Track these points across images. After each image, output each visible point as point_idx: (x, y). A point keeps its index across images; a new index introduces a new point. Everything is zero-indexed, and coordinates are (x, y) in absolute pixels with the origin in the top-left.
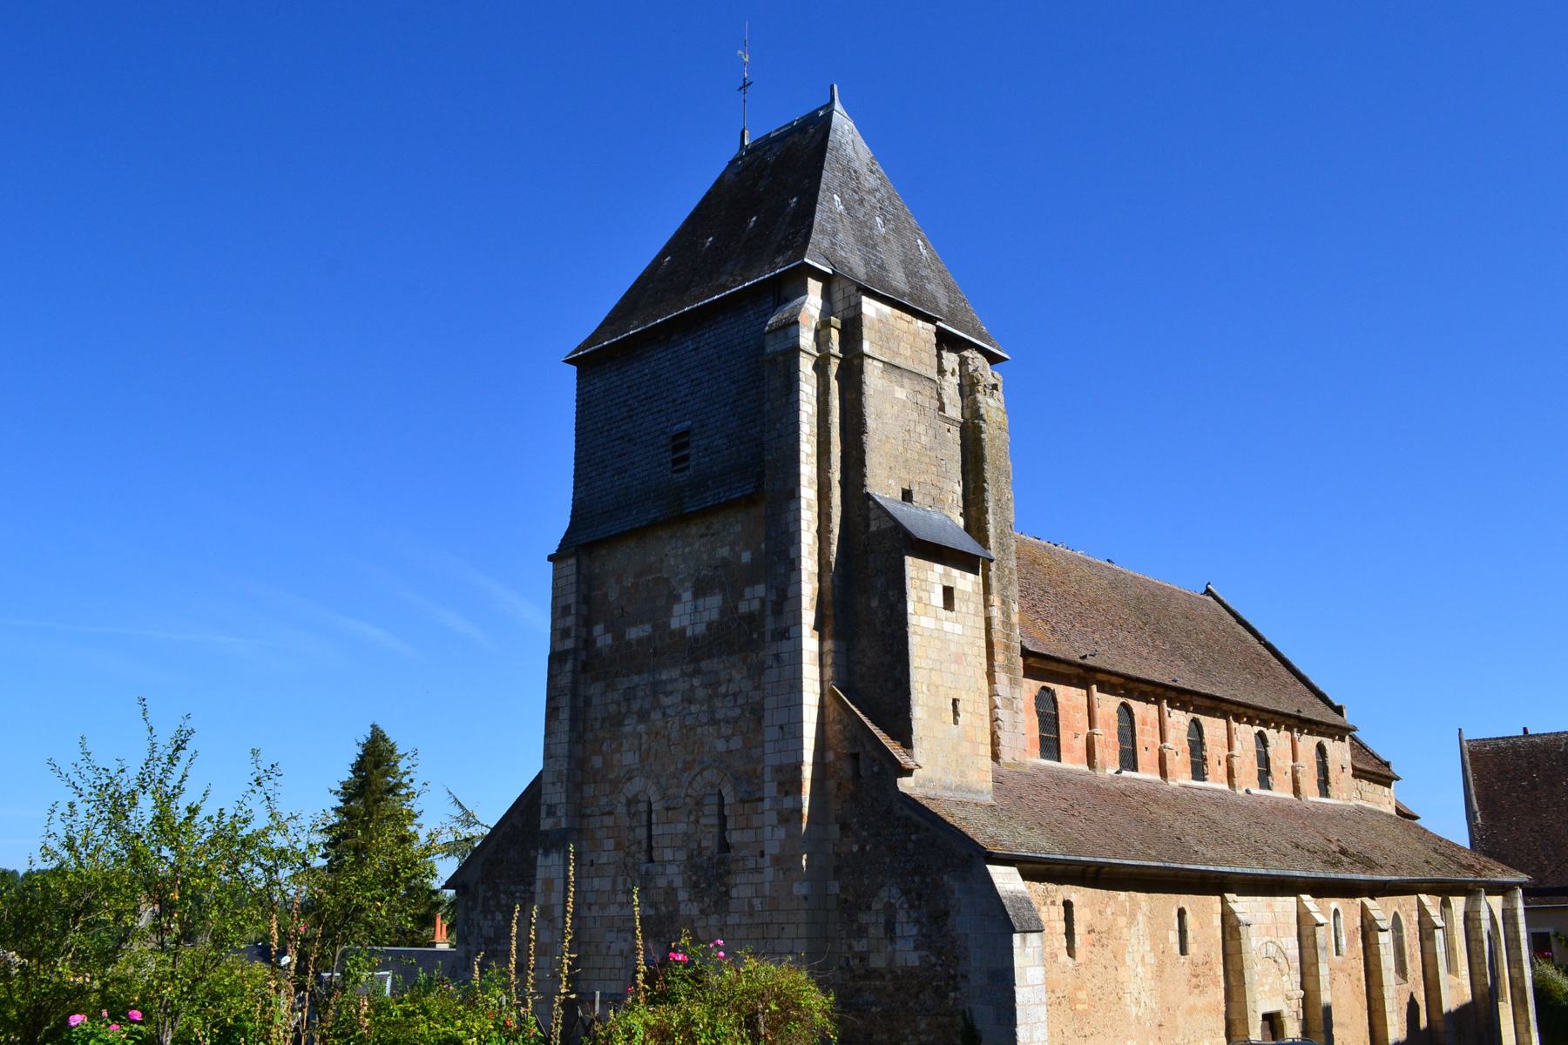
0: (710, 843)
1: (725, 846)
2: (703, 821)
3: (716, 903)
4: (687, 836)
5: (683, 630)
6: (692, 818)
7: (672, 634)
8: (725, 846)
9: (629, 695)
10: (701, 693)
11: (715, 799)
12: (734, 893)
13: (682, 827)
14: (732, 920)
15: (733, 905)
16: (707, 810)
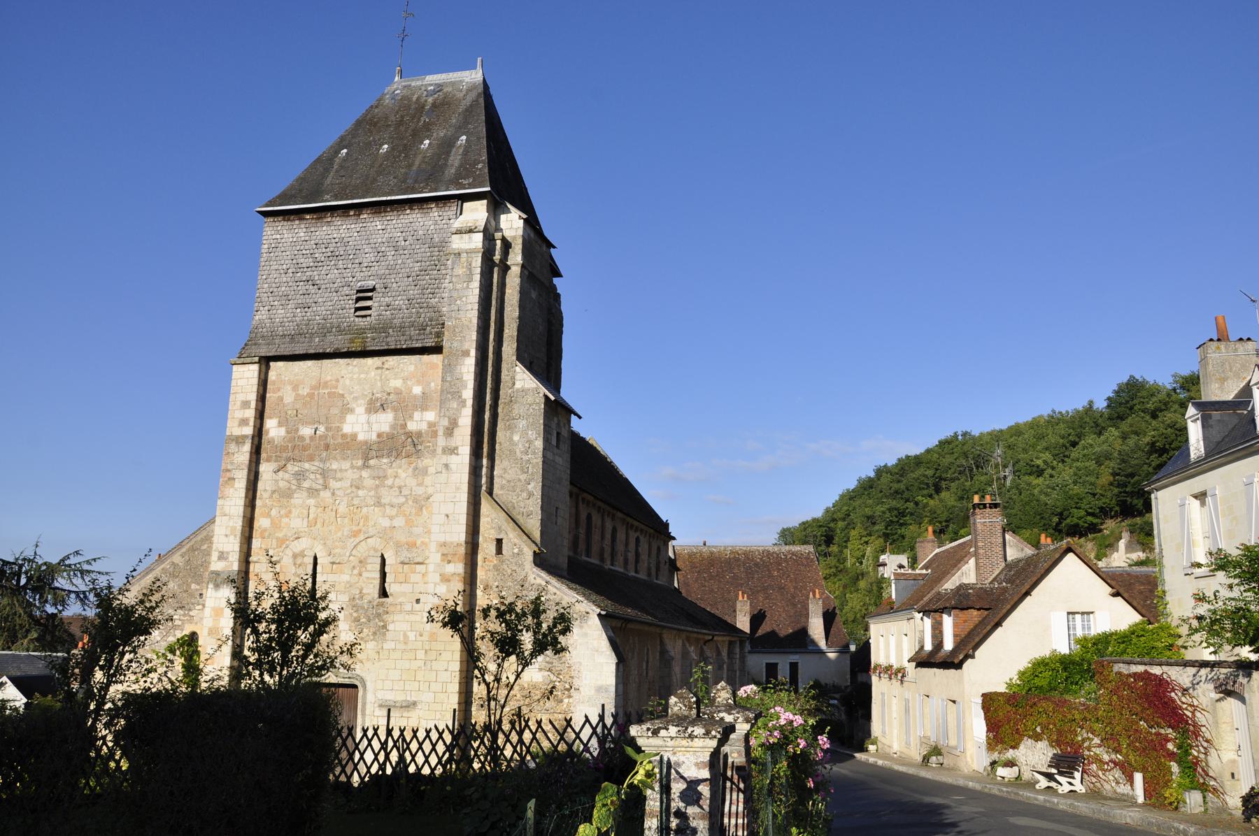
0: (373, 590)
1: (384, 593)
2: (365, 575)
3: (375, 634)
4: (350, 585)
5: (354, 436)
6: (356, 572)
7: (344, 436)
8: (384, 593)
9: (300, 476)
10: (369, 482)
11: (379, 560)
12: (390, 627)
13: (345, 578)
14: (389, 645)
15: (389, 635)
16: (369, 567)
